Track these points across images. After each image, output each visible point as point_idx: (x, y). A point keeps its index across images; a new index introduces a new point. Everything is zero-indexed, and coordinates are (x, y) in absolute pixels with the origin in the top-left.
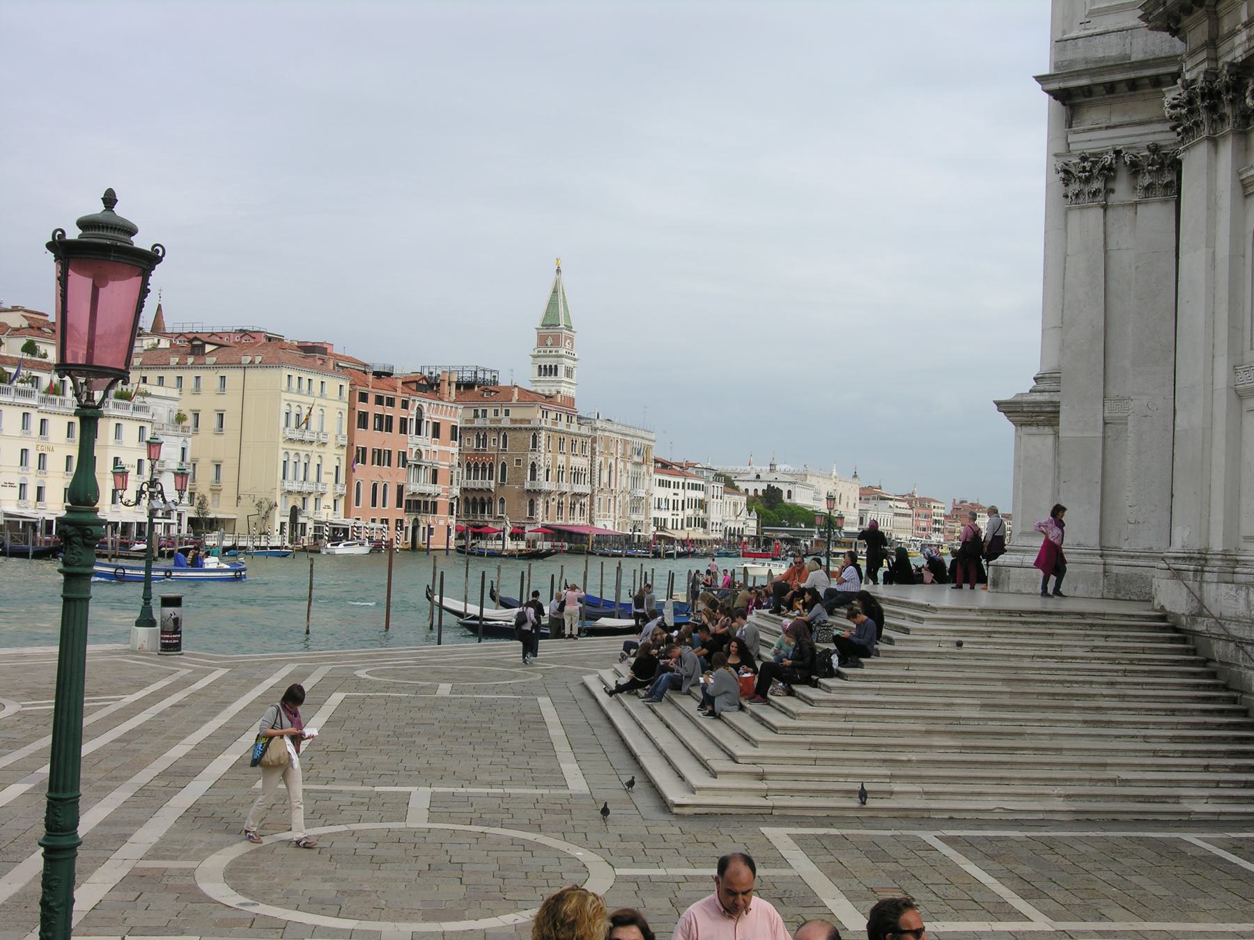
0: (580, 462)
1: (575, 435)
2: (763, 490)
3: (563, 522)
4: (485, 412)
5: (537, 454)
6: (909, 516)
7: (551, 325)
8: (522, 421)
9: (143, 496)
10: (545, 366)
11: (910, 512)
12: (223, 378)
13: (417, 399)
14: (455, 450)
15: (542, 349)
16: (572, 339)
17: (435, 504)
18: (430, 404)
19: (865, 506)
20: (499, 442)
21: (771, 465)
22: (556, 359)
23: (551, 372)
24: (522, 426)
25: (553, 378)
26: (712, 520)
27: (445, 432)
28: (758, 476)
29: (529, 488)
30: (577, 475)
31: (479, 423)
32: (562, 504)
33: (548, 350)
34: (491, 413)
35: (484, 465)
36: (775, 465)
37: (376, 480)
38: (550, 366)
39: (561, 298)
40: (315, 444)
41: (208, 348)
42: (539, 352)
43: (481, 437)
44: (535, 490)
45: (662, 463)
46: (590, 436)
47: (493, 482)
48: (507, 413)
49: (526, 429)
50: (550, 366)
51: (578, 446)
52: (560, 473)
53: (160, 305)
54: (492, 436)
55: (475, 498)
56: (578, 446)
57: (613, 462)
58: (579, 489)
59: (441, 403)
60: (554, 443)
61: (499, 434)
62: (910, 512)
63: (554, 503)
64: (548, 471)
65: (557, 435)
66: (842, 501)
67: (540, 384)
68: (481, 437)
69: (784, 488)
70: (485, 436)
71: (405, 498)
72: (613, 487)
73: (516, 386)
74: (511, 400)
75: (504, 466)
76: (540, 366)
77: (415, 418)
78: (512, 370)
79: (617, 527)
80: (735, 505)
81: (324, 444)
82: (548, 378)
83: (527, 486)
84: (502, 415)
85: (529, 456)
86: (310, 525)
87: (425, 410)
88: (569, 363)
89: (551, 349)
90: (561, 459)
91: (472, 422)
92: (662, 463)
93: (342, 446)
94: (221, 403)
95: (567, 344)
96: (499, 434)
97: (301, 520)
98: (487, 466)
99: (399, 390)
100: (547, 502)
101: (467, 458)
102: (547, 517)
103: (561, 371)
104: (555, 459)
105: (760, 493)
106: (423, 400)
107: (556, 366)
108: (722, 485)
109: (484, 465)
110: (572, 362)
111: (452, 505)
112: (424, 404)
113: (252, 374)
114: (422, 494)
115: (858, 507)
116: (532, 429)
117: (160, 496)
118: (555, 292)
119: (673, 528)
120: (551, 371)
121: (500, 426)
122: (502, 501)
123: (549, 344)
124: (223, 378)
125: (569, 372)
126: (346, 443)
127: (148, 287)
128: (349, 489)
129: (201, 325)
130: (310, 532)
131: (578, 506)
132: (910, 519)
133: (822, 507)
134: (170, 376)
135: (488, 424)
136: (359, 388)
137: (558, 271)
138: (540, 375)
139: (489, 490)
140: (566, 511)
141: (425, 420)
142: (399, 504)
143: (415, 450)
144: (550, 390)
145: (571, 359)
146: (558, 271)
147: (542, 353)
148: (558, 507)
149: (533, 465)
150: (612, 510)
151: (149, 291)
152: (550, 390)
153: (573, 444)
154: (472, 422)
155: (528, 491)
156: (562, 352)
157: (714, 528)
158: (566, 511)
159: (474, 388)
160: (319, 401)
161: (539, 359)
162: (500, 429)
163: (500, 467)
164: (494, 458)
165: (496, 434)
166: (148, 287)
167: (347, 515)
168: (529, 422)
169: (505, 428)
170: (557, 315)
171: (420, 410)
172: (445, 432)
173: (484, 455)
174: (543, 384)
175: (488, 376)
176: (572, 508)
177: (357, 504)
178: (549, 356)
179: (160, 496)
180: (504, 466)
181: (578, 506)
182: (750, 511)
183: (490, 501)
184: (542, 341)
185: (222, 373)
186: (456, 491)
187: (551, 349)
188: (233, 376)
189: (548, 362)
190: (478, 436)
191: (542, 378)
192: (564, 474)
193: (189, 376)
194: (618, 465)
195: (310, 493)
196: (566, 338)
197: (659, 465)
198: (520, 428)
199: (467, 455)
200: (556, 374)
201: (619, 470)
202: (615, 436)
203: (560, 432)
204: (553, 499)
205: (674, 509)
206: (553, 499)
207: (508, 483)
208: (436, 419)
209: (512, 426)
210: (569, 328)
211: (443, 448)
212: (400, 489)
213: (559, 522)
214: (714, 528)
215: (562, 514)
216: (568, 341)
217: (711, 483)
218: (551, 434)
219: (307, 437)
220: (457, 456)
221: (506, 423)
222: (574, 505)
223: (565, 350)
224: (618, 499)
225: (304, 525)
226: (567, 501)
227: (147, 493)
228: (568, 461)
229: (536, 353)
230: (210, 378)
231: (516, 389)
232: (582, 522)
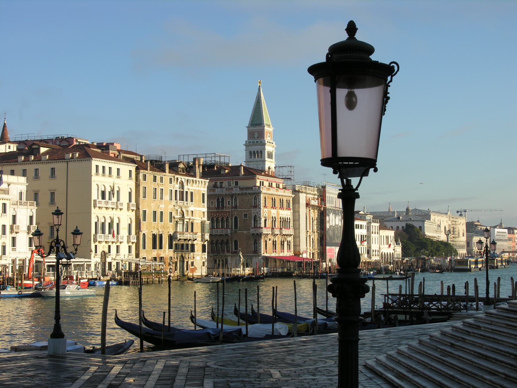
0: (287, 214)
1: (282, 196)
2: (403, 227)
3: (277, 255)
4: (221, 183)
5: (257, 210)
8: (247, 188)
9: (53, 250)
12: (53, 170)
13: (179, 177)
14: (205, 210)
15: (251, 141)
17: (193, 246)
18: (188, 180)
20: (232, 203)
22: (261, 146)
24: (248, 192)
26: (372, 248)
27: (197, 198)
28: (399, 218)
29: (254, 232)
30: (285, 222)
31: (218, 191)
32: (276, 242)
33: (255, 141)
34: (225, 184)
35: (222, 219)
37: (155, 232)
40: (114, 210)
41: (43, 150)
42: (250, 142)
43: (220, 200)
44: (257, 234)
46: (291, 197)
47: (229, 231)
48: (237, 183)
49: (249, 194)
51: (285, 203)
52: (274, 221)
53: (5, 123)
54: (227, 200)
55: (218, 241)
56: (285, 203)
58: (285, 231)
59: (194, 179)
60: (269, 203)
61: (232, 197)
63: (270, 242)
64: (265, 220)
65: (270, 196)
68: (220, 200)
69: (417, 225)
70: (223, 199)
71: (174, 243)
72: (308, 230)
73: (241, 166)
74: (239, 175)
75: (236, 219)
76: (251, 152)
77: (178, 190)
79: (311, 256)
80: (387, 237)
81: (121, 209)
83: (252, 231)
84: (233, 184)
85: (253, 211)
86: (114, 263)
87: (185, 184)
89: (257, 140)
90: (274, 212)
91: (214, 191)
93: (133, 210)
94: (53, 184)
96: (232, 197)
97: (108, 260)
98: (225, 219)
99: (167, 170)
100: (266, 242)
101: (211, 214)
102: (266, 252)
104: (270, 213)
105: (400, 228)
106: (183, 177)
107: (261, 152)
108: (378, 225)
109: (222, 219)
111: (204, 246)
112: (183, 180)
113: (71, 164)
114: (185, 240)
116: (254, 194)
117: (63, 249)
121: (233, 193)
122: (236, 242)
123: (256, 136)
124: (53, 170)
126: (135, 208)
127: (388, 95)
128: (138, 238)
129: (33, 135)
130: (114, 269)
131: (286, 243)
133: (443, 237)
134: (18, 168)
135: (225, 192)
136: (141, 171)
138: (251, 158)
139: (227, 235)
140: (278, 246)
141: (185, 190)
142: (170, 247)
143: (179, 210)
148: (273, 244)
149: (255, 217)
150: (308, 244)
151: (389, 98)
153: (281, 201)
154: (214, 191)
155: (253, 234)
157: (374, 253)
158: (278, 246)
159: (214, 168)
160: (117, 181)
161: (250, 147)
162: (233, 194)
163: (233, 219)
164: (229, 215)
165: (230, 198)
166: (388, 95)
167: (137, 256)
168: (252, 188)
169: (235, 194)
171: (182, 184)
172: (197, 198)
173: (223, 212)
175: (222, 160)
176: (282, 244)
177: (144, 247)
179: (63, 249)
180: (236, 219)
181: (286, 243)
182: (396, 241)
183: (227, 243)
184: (251, 135)
185: (53, 165)
186: (207, 237)
187: (257, 140)
188: (60, 166)
190: (218, 200)
192: (276, 222)
193: (30, 168)
195: (113, 242)
198: (246, 193)
199: (212, 213)
201: (311, 218)
203: (272, 194)
204: (270, 239)
206: (270, 239)
207: (239, 230)
208: (192, 189)
209: (240, 192)
211: (198, 209)
212: (171, 238)
213: (273, 255)
214: (374, 253)
215: (275, 249)
218: (266, 196)
219: (110, 206)
220: (206, 214)
221: (236, 191)
222: (284, 242)
224: (311, 237)
225: (110, 264)
226: (278, 239)
227: (55, 248)
228: (278, 213)
230: (45, 169)
231: (242, 167)
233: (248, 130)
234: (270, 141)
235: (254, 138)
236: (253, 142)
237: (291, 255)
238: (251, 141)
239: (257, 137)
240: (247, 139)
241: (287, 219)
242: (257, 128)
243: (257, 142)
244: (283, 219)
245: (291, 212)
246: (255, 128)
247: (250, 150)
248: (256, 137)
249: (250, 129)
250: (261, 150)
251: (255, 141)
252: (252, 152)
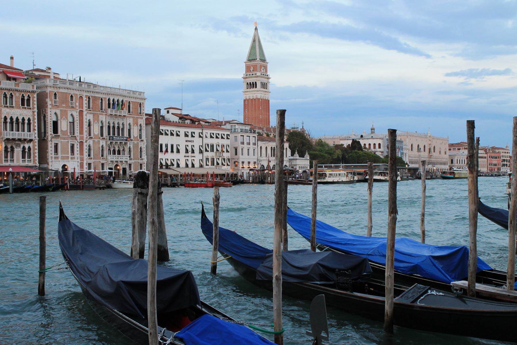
6: (485, 158)
7: (252, 60)
10: (250, 83)
11: (486, 155)
15: (248, 74)
16: (266, 68)
19: (452, 152)
21: (372, 129)
23: (253, 86)
25: (254, 89)
33: (251, 74)
36: (373, 129)
38: (253, 83)
39: (257, 44)
42: (246, 75)
45: (191, 120)
50: (253, 83)
57: (76, 115)
62: (486, 155)
66: (436, 150)
67: (248, 93)
78: (33, 54)
82: (252, 89)
88: (264, 80)
89: (253, 73)
92: (191, 120)
95: (261, 69)
103: (259, 85)
107: (256, 82)
110: (266, 80)
115: (449, 153)
118: (254, 41)
119: (187, 165)
120: (253, 85)
123: (252, 70)
125: (264, 86)
132: (486, 160)
137: (256, 29)
144: (253, 96)
145: (265, 78)
146: (256, 29)
147: (248, 76)
152: (253, 96)
156: (258, 74)
161: (247, 79)
170: (255, 54)
174: (250, 93)
178: (252, 77)
184: (248, 69)
189: (251, 80)
191: (248, 90)
194: (85, 117)
196: (261, 67)
197: (188, 122)
200: (256, 87)
202: (77, 93)
205: (187, 151)
210: (264, 60)
216: (262, 68)
217: (239, 133)
223: (260, 73)
229: (245, 76)
232: (26, 163)
233: (246, 65)
234: (264, 74)
235: (251, 71)
236: (250, 75)
237: (31, 164)
238: (248, 74)
239: (253, 71)
240: (245, 73)
241: (23, 119)
242: (253, 63)
243: (252, 74)
244: (11, 119)
245: (33, 112)
246: (251, 63)
247: (247, 82)
248: (252, 70)
249: (247, 63)
250: (255, 81)
251: (251, 74)
252: (249, 83)
